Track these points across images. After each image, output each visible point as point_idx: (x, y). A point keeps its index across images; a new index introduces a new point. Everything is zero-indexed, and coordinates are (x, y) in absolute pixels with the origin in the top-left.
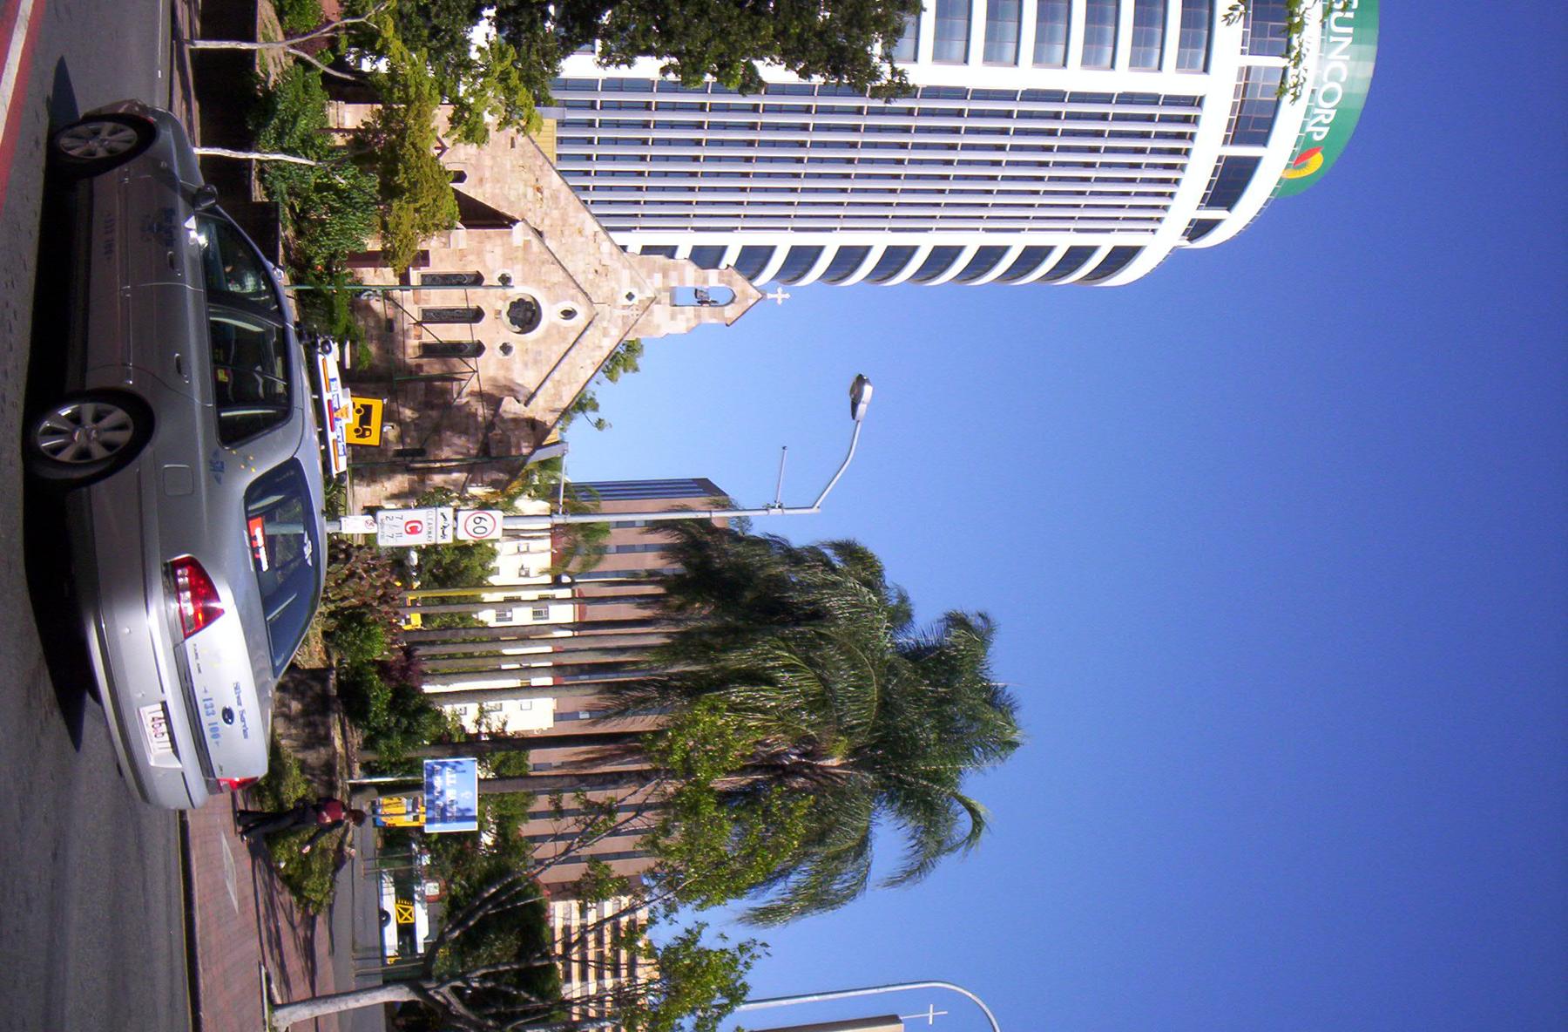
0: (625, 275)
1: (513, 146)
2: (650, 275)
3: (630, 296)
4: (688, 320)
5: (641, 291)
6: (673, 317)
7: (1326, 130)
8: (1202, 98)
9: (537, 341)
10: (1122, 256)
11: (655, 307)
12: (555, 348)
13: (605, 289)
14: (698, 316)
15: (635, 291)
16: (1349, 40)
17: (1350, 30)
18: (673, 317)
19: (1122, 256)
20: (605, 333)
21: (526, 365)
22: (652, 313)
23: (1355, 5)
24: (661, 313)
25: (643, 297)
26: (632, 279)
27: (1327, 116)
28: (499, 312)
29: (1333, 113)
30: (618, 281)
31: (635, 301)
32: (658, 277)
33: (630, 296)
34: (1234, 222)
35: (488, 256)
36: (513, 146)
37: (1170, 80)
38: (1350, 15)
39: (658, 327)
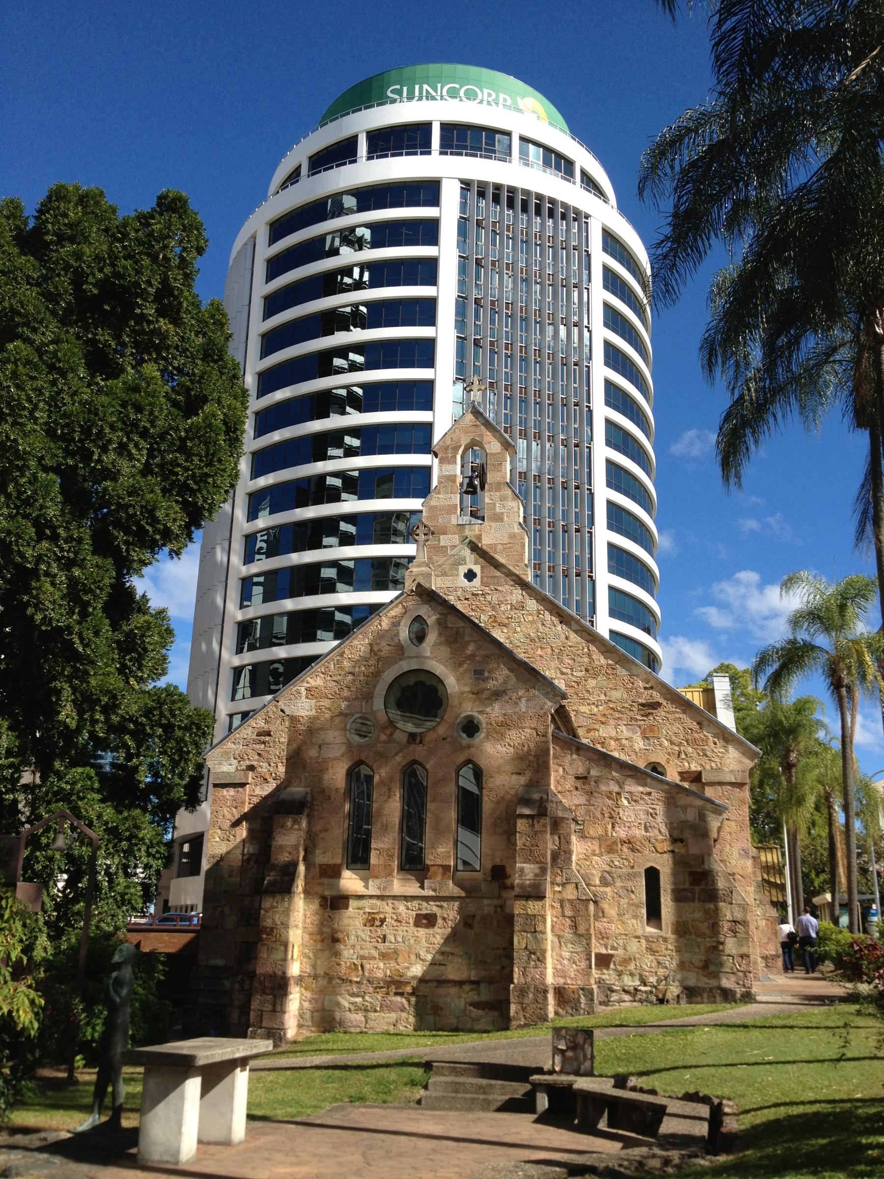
1: (268, 734)
3: (470, 575)
4: (503, 499)
6: (498, 518)
7: (502, 96)
8: (462, 181)
10: (613, 243)
11: (486, 542)
14: (498, 486)
15: (463, 570)
16: (425, 87)
17: (417, 87)
18: (498, 518)
19: (613, 243)
20: (522, 607)
23: (398, 87)
24: (490, 536)
26: (444, 574)
27: (489, 95)
28: (412, 736)
29: (486, 91)
31: (477, 569)
33: (470, 575)
34: (584, 159)
36: (268, 734)
37: (448, 212)
38: (405, 89)
39: (513, 536)
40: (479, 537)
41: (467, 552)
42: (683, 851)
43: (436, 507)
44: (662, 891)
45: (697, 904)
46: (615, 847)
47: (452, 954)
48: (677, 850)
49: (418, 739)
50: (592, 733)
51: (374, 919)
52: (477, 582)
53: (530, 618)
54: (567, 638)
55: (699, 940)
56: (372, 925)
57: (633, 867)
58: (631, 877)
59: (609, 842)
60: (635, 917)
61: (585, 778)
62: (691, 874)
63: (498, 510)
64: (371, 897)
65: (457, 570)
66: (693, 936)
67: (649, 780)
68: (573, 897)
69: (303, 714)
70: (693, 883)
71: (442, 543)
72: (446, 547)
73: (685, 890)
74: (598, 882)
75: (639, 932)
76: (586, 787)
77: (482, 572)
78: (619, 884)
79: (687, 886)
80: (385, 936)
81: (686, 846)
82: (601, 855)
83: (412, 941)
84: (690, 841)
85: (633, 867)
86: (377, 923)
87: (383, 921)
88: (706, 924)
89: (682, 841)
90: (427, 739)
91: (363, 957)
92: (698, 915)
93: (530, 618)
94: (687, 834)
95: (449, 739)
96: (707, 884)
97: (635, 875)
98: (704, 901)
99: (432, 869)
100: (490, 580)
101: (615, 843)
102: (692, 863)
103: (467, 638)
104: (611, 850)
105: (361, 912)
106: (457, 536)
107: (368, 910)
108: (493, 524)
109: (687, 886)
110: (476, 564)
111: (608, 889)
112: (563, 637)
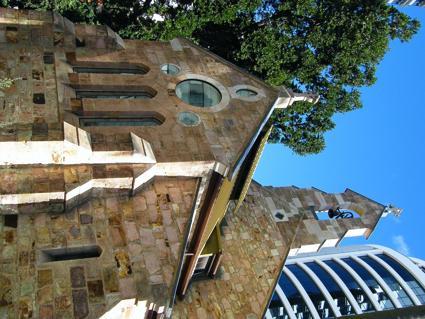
0: (269, 200)
2: (289, 199)
4: (336, 229)
5: (288, 211)
9: (223, 112)
12: (246, 118)
13: (256, 212)
15: (282, 212)
20: (271, 246)
21: (218, 132)
22: (303, 226)
25: (291, 215)
26: (275, 203)
30: (266, 206)
31: (285, 219)
32: (296, 200)
35: (150, 56)
40: (305, 218)
41: (294, 212)
42: (120, 274)
43: (314, 194)
44: (80, 260)
45: (71, 289)
46: (114, 223)
47: (13, 112)
48: (120, 269)
49: (173, 94)
50: (197, 302)
51: (39, 75)
52: (278, 220)
53: (266, 253)
54: (260, 277)
55: (33, 295)
56: (33, 74)
57: (99, 237)
58: (90, 236)
59: (118, 218)
60: (53, 241)
61: (169, 201)
62: (100, 282)
63: (327, 227)
64: (55, 73)
65: (280, 208)
66: (37, 289)
67: (180, 255)
68: (66, 181)
69: (172, 47)
70: (90, 284)
71: (293, 199)
72: (292, 201)
73: (84, 278)
74: (82, 213)
75: (37, 245)
76: (161, 203)
77: (285, 222)
78: (83, 228)
79: (87, 280)
80: (26, 79)
81: (125, 276)
82: (106, 214)
83: (23, 92)
84: (131, 280)
85: (99, 237)
86: (35, 76)
87: (38, 79)
88: (50, 299)
89: (130, 272)
90: (173, 98)
91: (9, 70)
92: (59, 292)
93: (266, 253)
94: (137, 277)
95: (177, 108)
96: (92, 296)
97: (92, 239)
98: (73, 296)
99: (79, 102)
100: (281, 227)
101: (119, 223)
102: (111, 282)
103: (252, 116)
104: (111, 221)
105: (44, 69)
106: (301, 206)
107: (44, 72)
108: (318, 225)
109: (87, 280)
110: (289, 218)
111: (76, 220)
112: (260, 275)
